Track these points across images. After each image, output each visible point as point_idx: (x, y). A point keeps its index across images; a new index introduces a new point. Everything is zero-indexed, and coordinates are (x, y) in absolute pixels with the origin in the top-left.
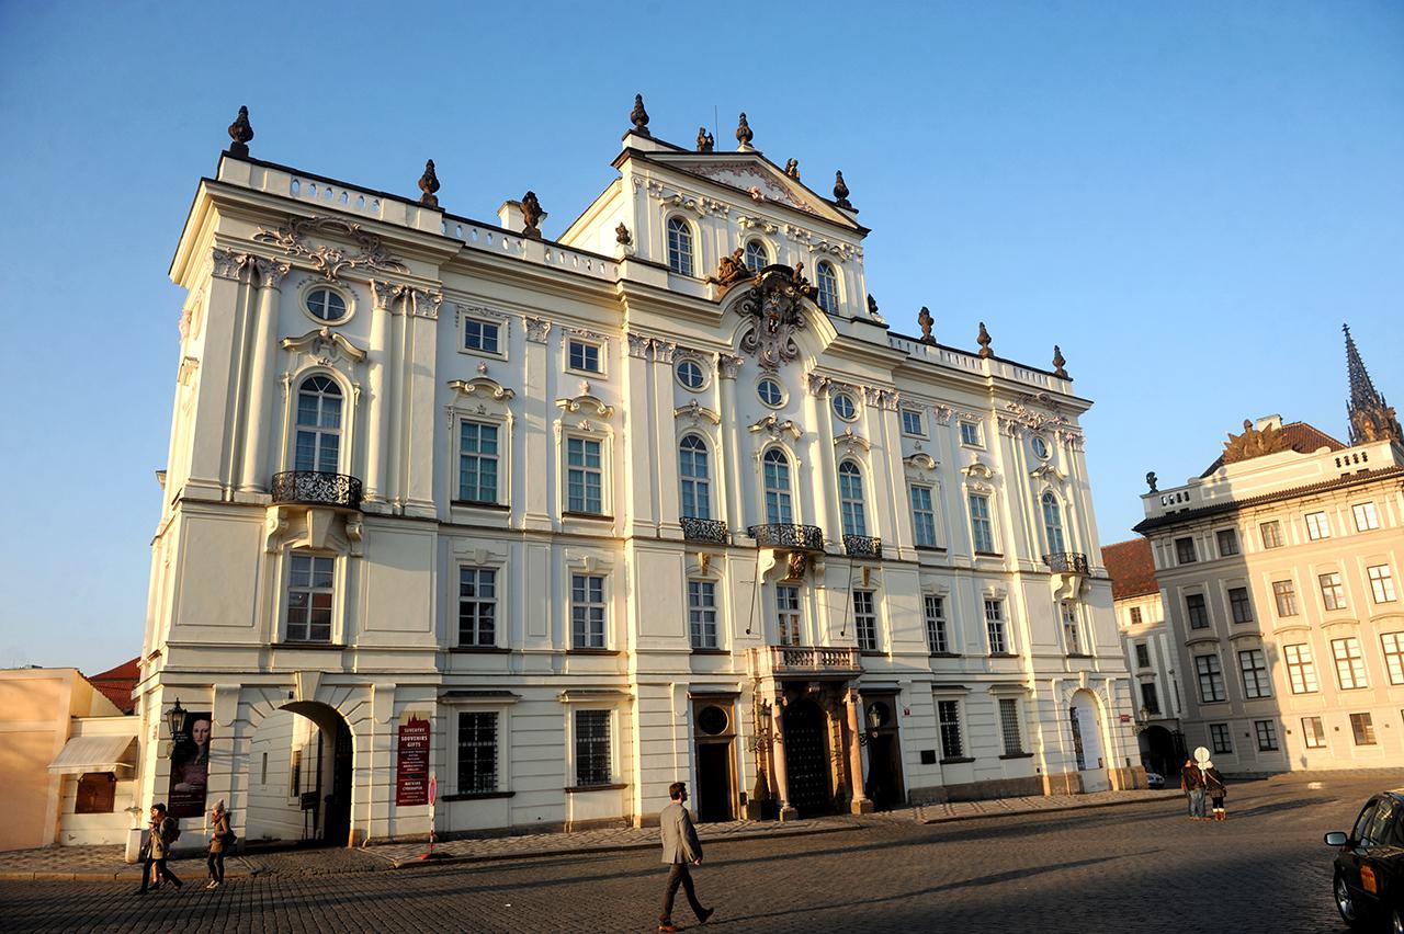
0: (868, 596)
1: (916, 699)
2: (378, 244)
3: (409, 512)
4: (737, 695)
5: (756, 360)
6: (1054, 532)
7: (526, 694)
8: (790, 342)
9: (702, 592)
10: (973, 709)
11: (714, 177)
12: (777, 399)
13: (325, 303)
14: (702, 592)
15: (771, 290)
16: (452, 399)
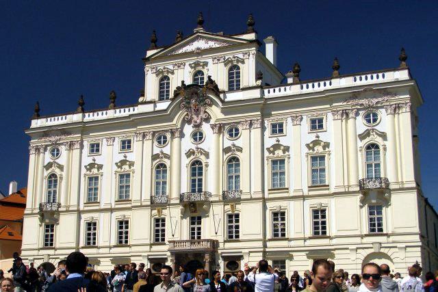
0: (237, 216)
1: (251, 259)
2: (64, 131)
3: (71, 209)
4: (166, 259)
5: (192, 125)
6: (373, 166)
7: (101, 260)
8: (205, 112)
9: (159, 222)
10: (292, 263)
11: (180, 51)
12: (201, 139)
13: (56, 153)
14: (159, 222)
15: (192, 94)
16: (84, 171)
